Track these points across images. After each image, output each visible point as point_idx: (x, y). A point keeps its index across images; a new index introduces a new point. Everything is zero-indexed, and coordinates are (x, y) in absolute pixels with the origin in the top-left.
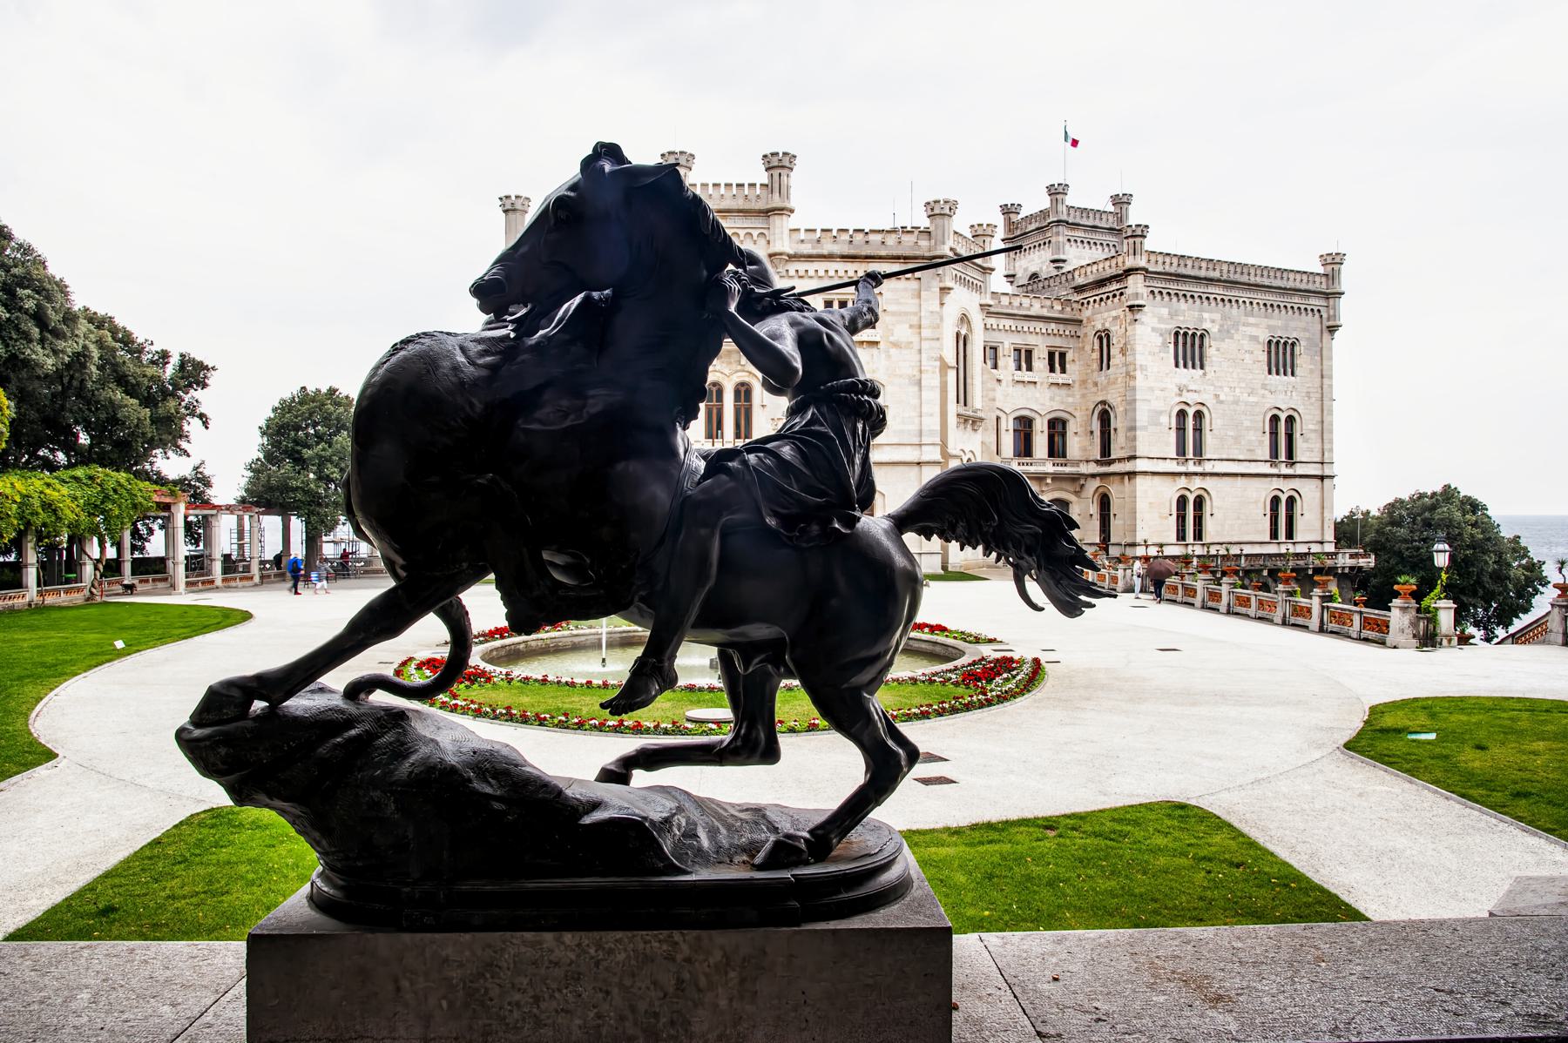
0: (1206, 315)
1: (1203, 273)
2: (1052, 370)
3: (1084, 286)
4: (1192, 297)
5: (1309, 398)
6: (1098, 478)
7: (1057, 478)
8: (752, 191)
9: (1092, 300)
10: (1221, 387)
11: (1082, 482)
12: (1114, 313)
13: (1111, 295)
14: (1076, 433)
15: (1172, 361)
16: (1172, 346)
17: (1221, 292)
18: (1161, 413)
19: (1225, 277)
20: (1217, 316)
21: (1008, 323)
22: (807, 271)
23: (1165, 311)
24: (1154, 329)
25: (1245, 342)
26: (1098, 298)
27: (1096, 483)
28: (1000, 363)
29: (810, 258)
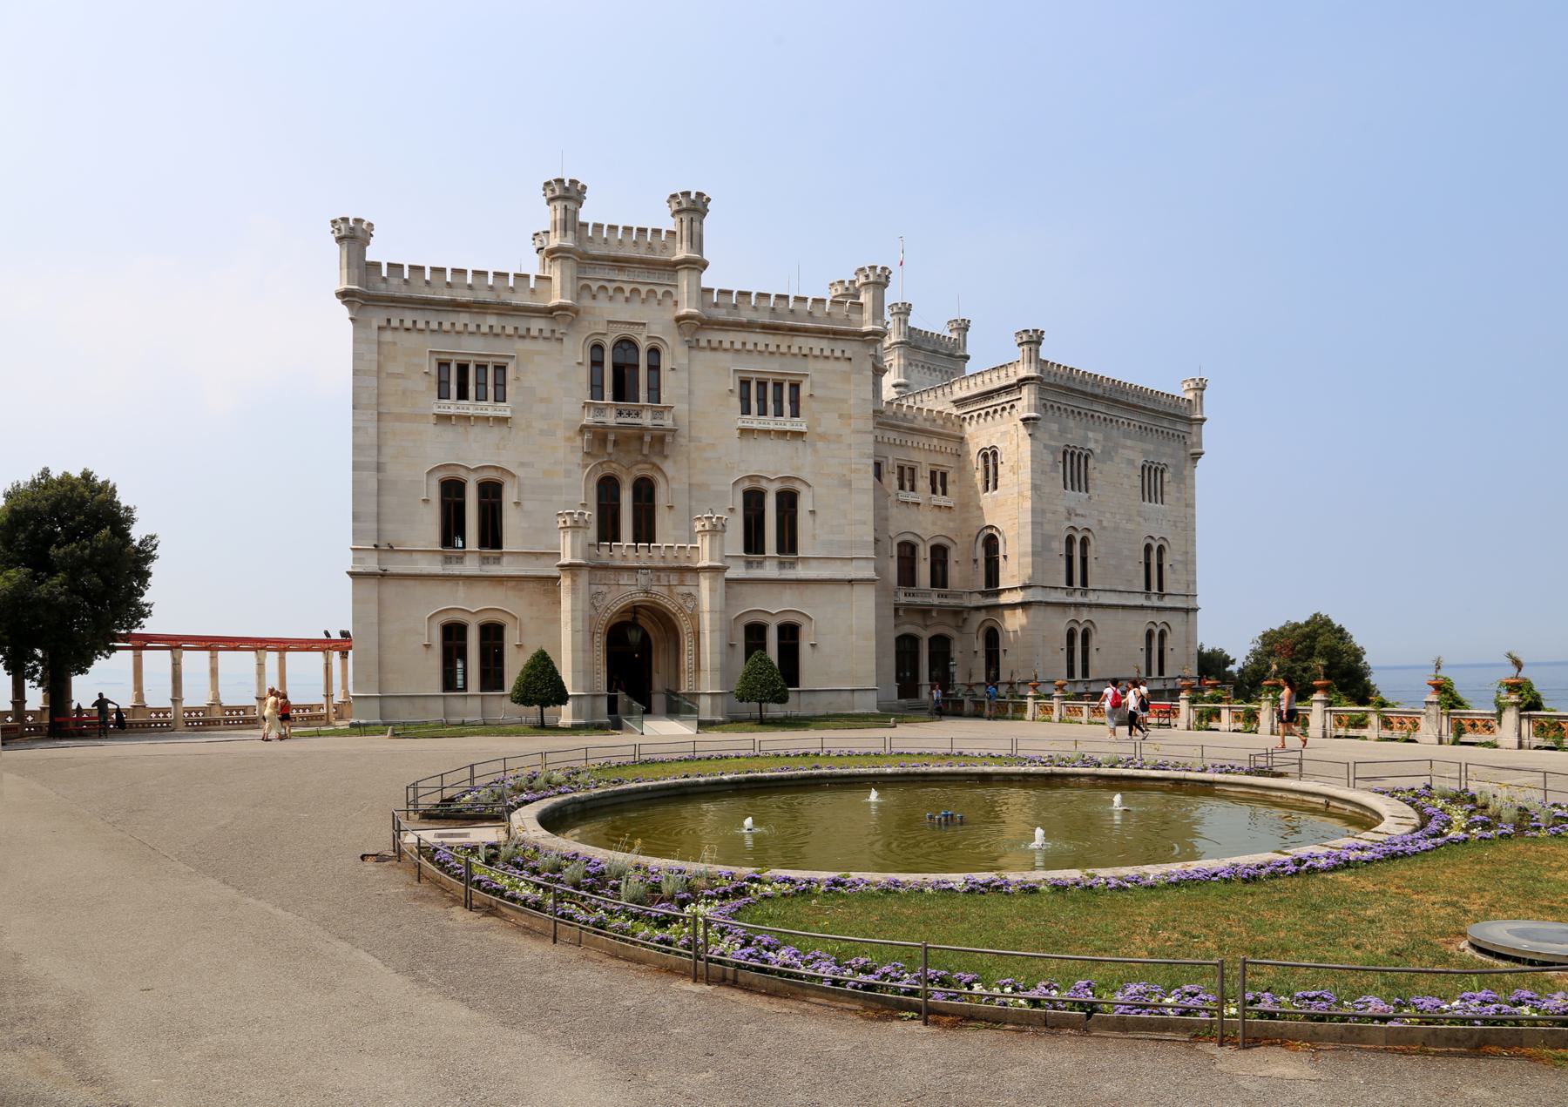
0: (1091, 435)
1: (1089, 389)
2: (934, 491)
3: (966, 399)
4: (1079, 413)
5: (1176, 527)
6: (983, 611)
7: (942, 610)
8: (656, 239)
9: (975, 414)
10: (1104, 512)
11: (965, 616)
12: (1003, 428)
13: (999, 408)
14: (957, 562)
15: (1062, 482)
16: (1061, 465)
17: (1104, 411)
18: (1052, 538)
19: (1107, 395)
20: (1100, 436)
21: (892, 435)
22: (721, 342)
23: (1055, 427)
25: (1123, 466)
26: (983, 412)
27: (982, 616)
28: (885, 480)
29: (725, 326)
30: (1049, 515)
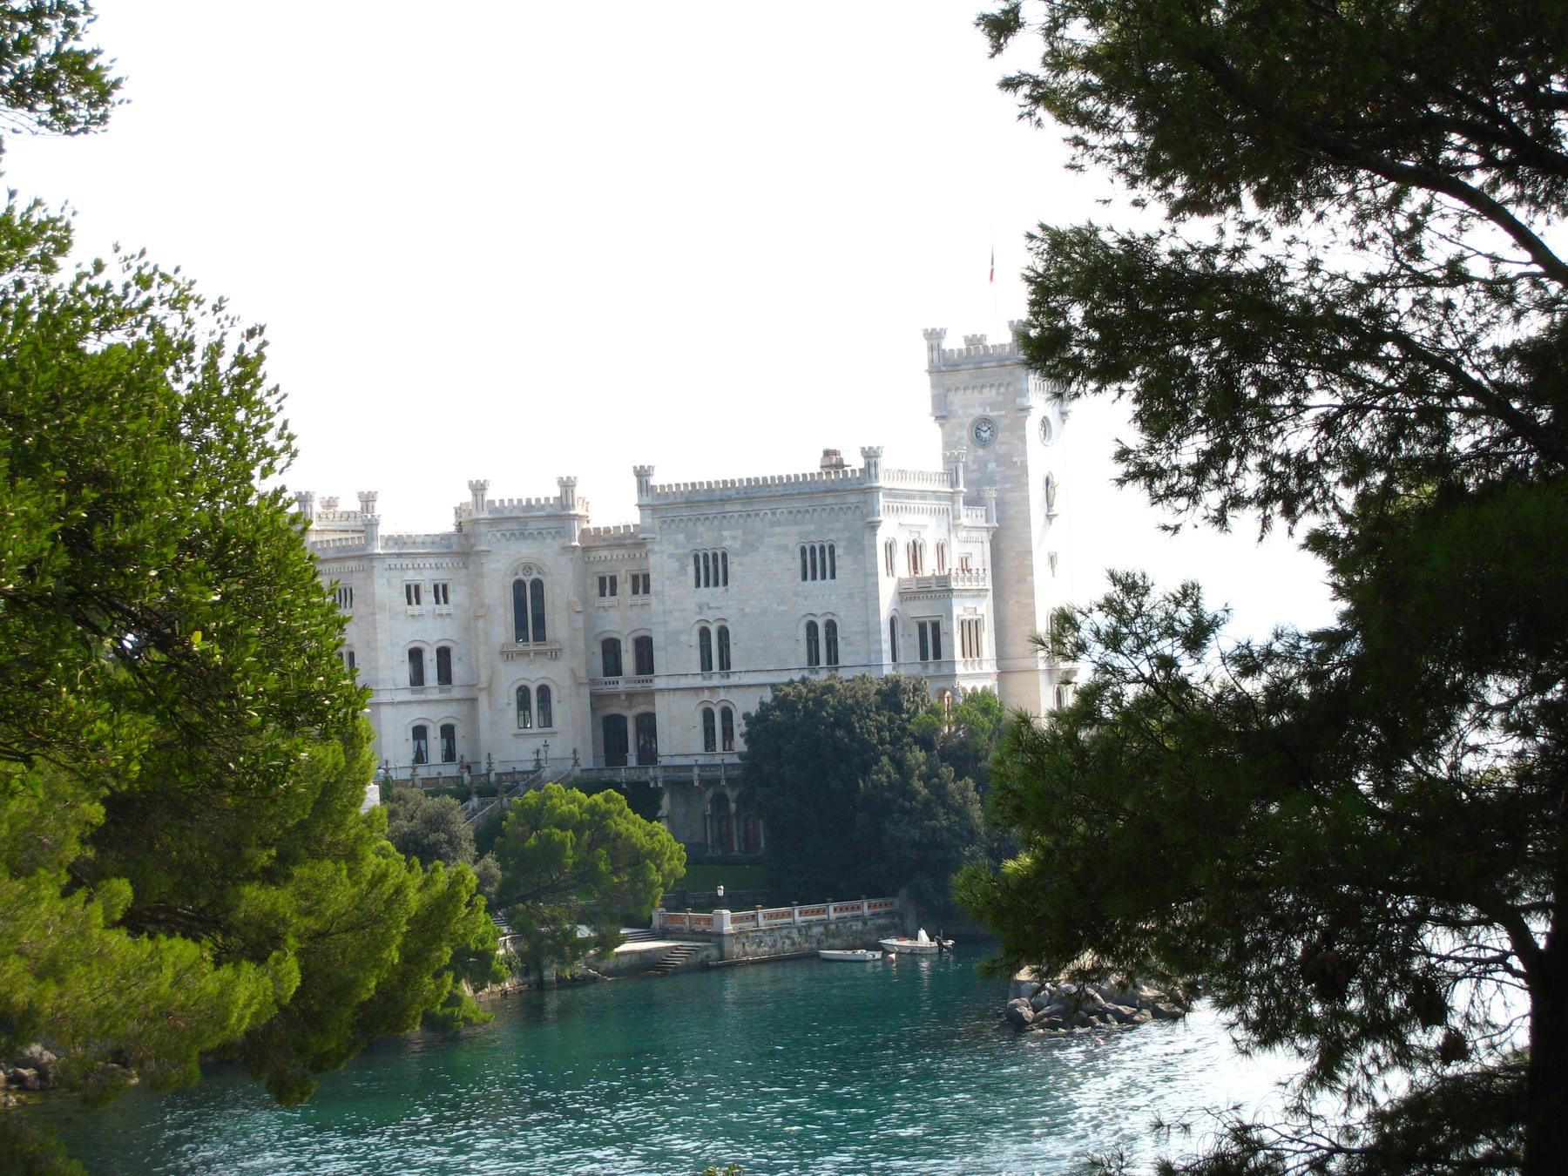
0: (725, 533)
15: (692, 581)
16: (691, 570)
20: (739, 533)
21: (620, 553)
23: (681, 537)
24: (671, 556)
30: (677, 614)
